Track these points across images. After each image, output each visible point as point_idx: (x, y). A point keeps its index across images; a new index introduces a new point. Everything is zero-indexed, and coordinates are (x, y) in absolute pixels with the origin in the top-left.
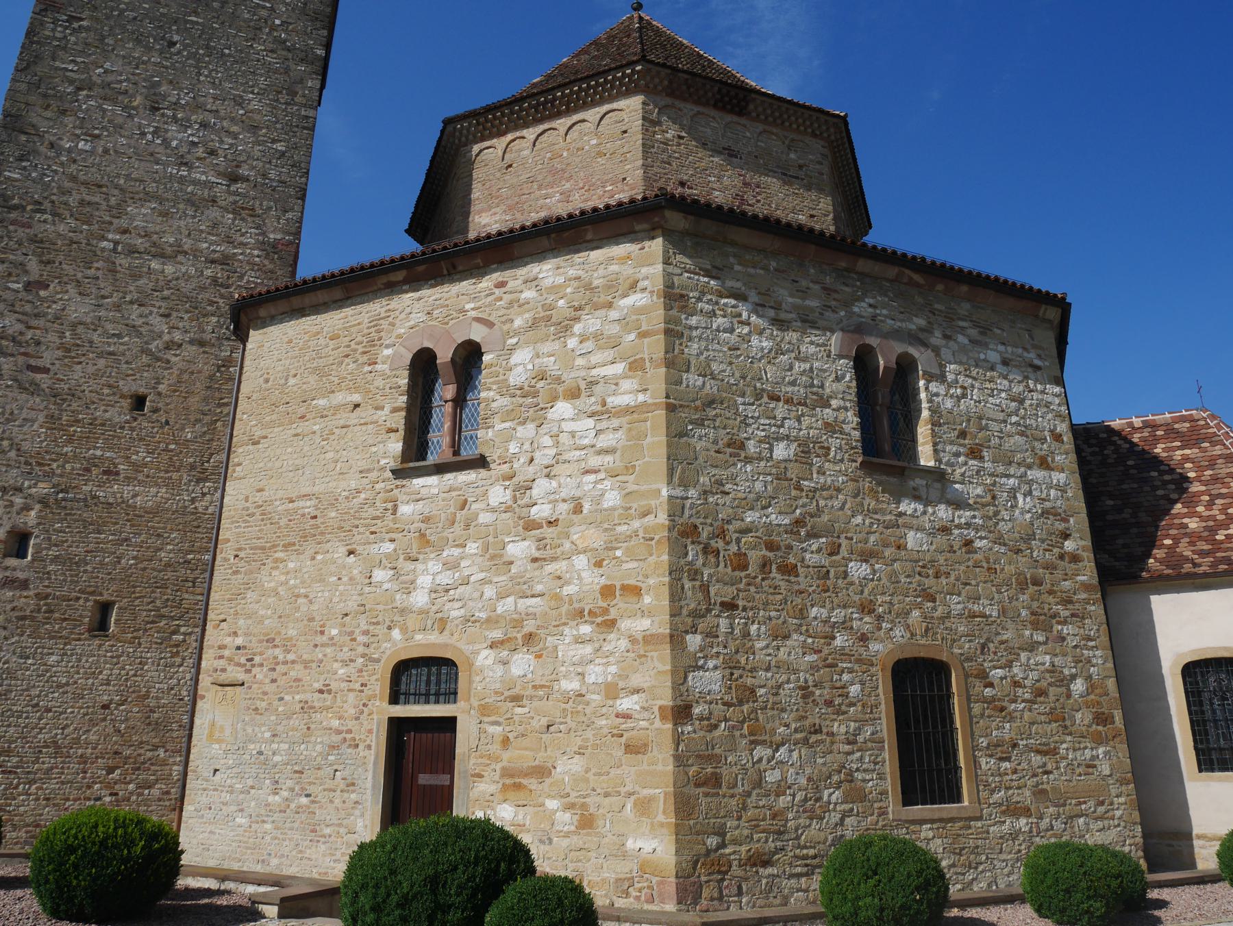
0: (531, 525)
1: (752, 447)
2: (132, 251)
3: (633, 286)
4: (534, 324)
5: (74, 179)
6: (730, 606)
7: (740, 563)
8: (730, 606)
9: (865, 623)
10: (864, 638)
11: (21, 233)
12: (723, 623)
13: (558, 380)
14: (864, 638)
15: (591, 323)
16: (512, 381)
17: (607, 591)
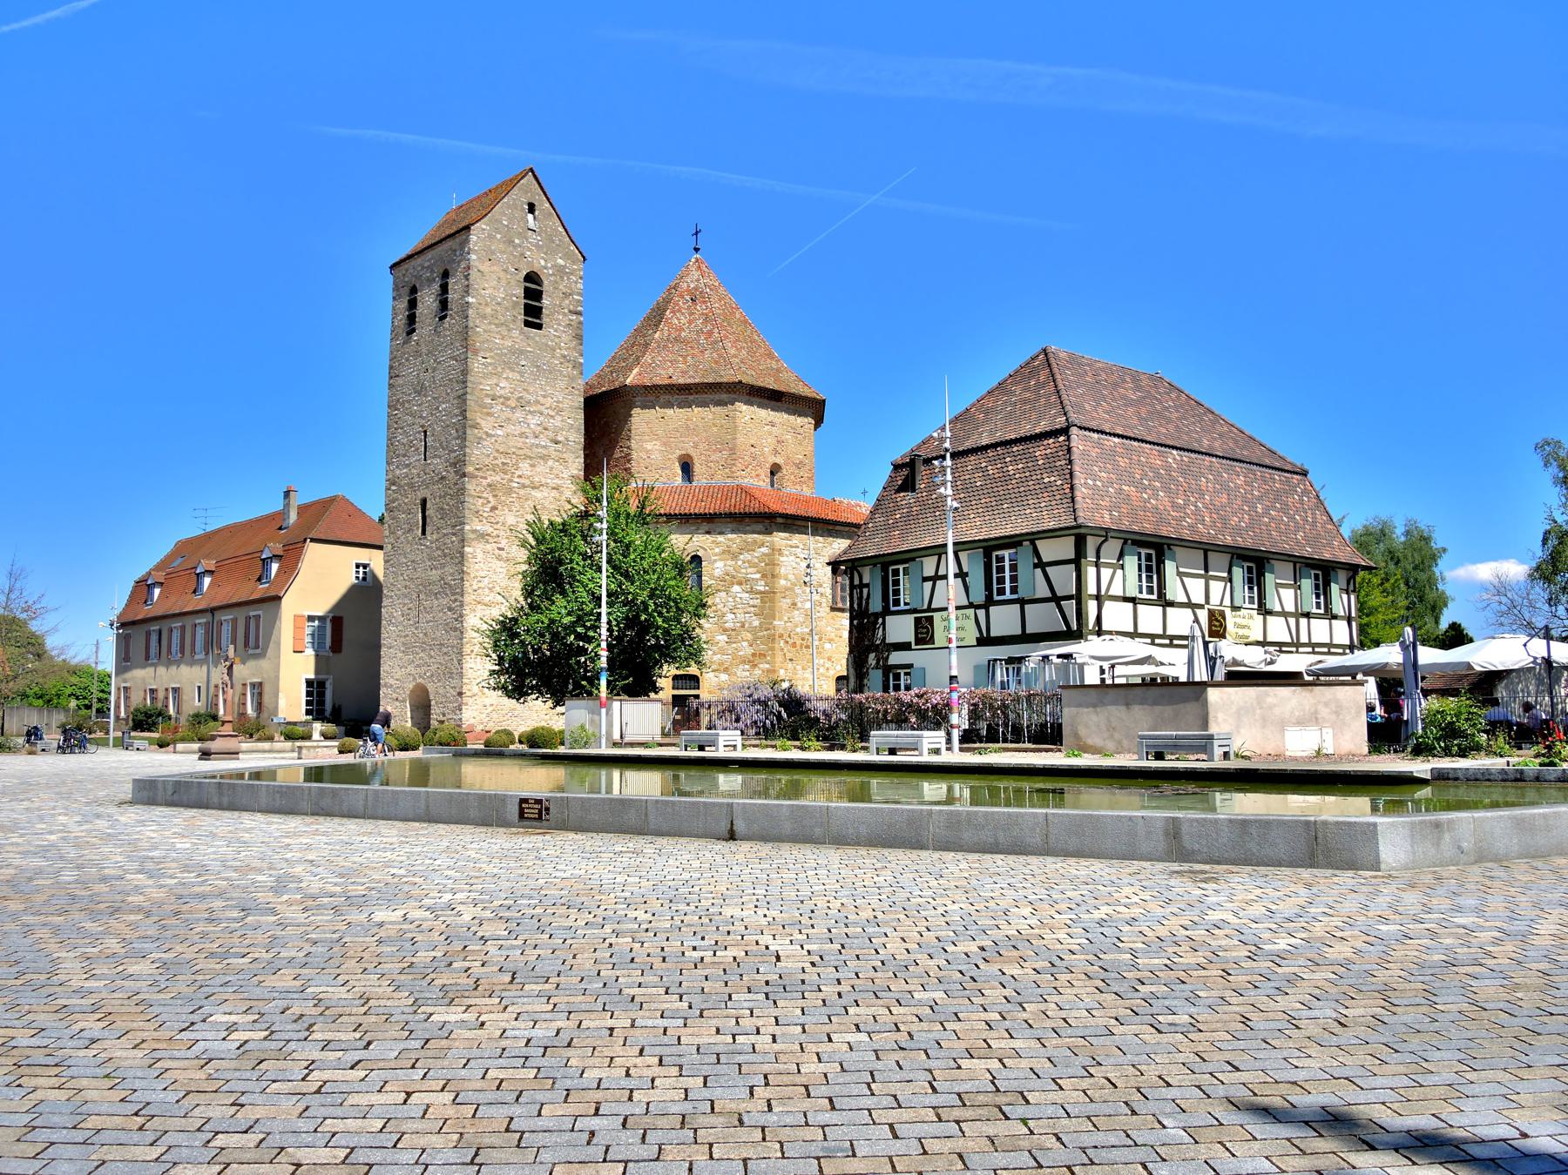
0: (725, 630)
1: (799, 605)
2: (524, 486)
3: (763, 545)
4: (724, 552)
5: (497, 451)
6: (791, 660)
7: (794, 645)
8: (791, 660)
9: (828, 664)
10: (828, 669)
11: (485, 482)
12: (790, 665)
13: (733, 577)
14: (828, 669)
15: (746, 556)
16: (716, 575)
17: (754, 655)
